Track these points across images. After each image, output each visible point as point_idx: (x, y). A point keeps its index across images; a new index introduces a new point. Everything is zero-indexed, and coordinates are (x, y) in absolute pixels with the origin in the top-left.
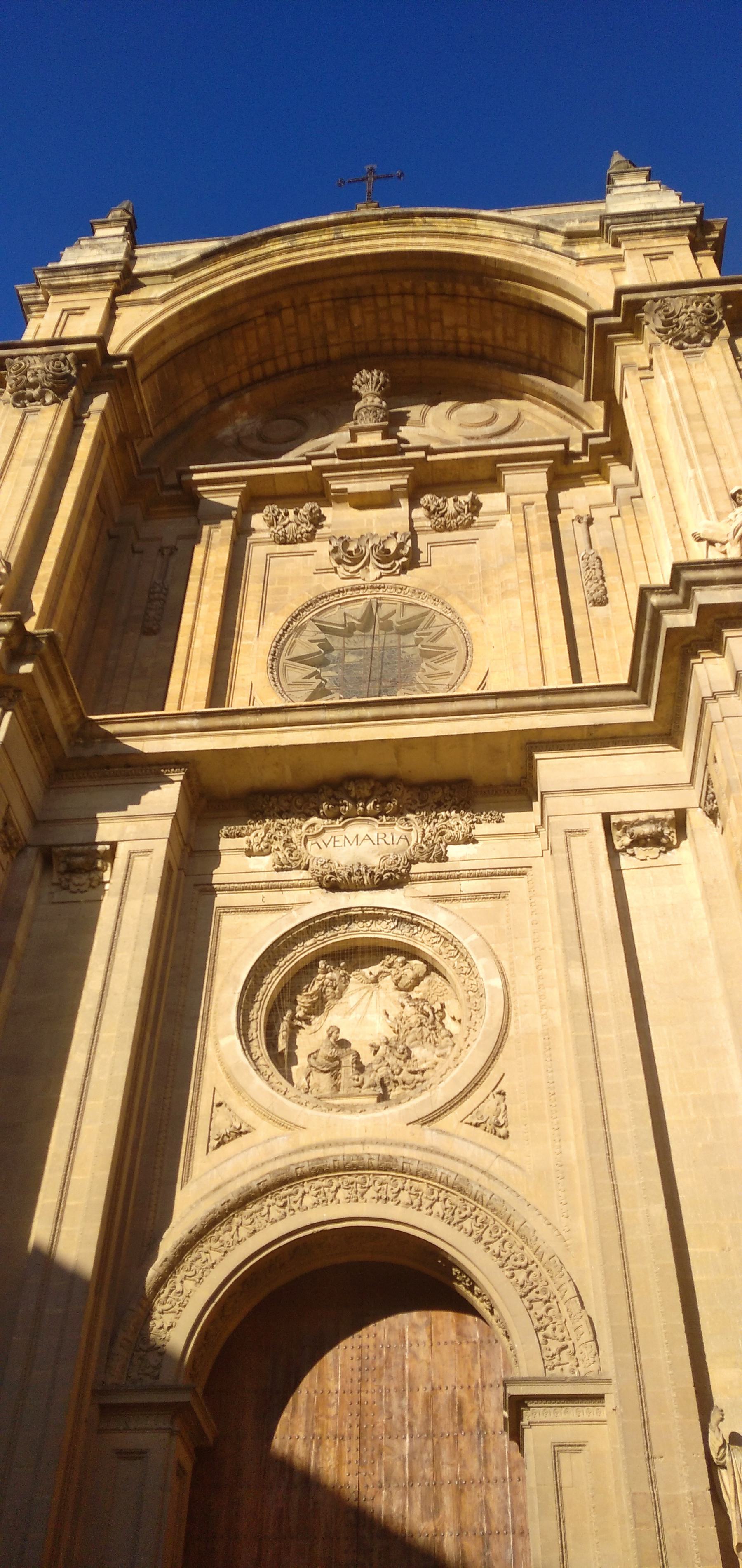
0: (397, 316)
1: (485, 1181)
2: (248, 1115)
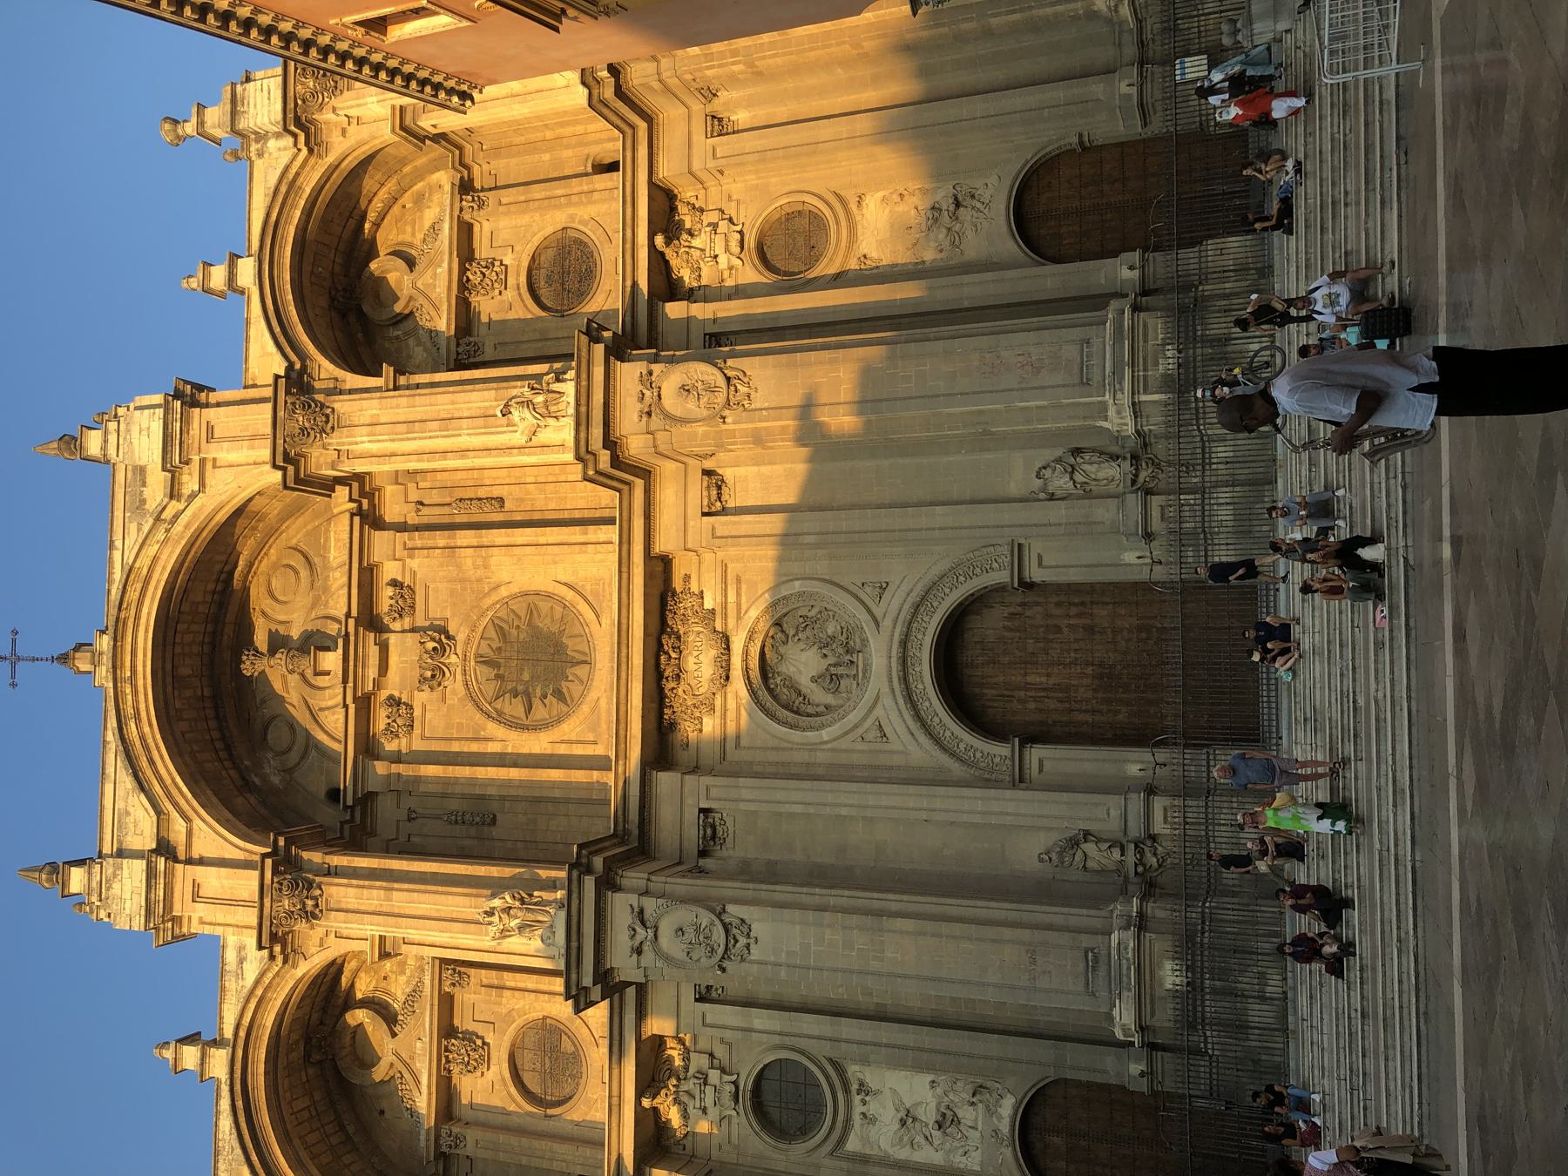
0: (188, 638)
1: (913, 594)
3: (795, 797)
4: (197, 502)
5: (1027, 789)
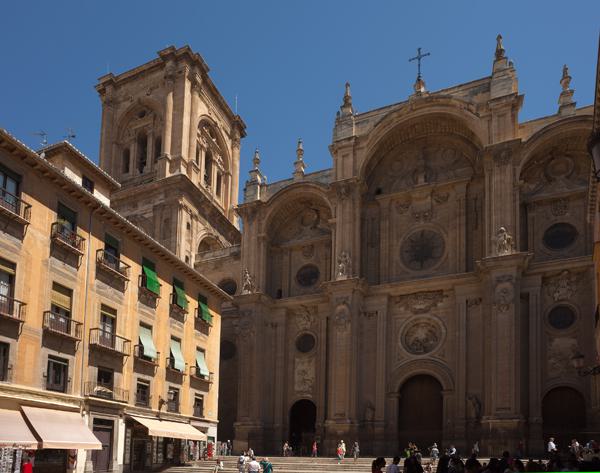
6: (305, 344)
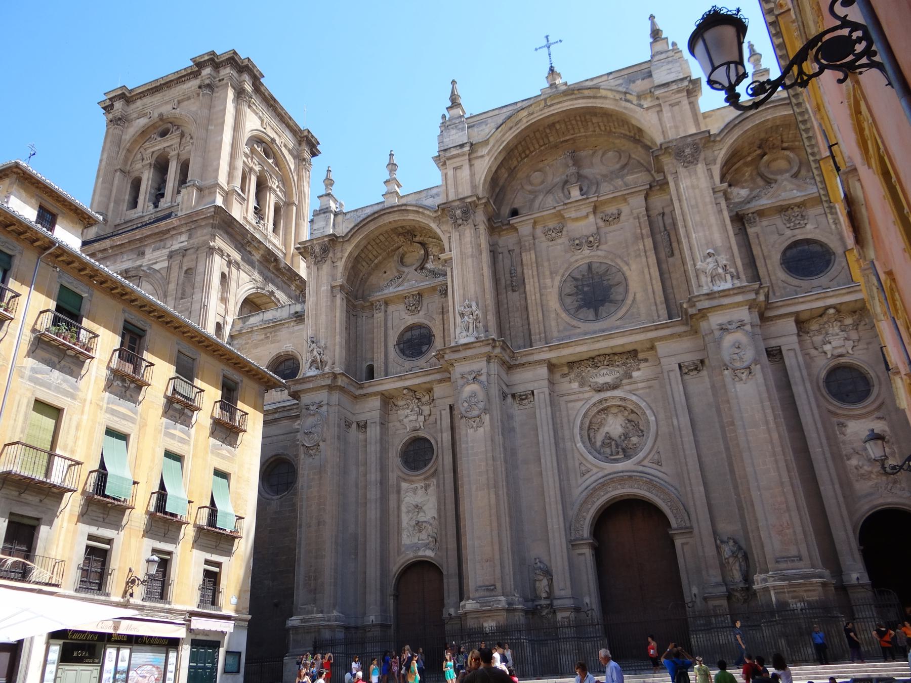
2: (589, 466)
3: (545, 435)
4: (638, 109)
5: (568, 549)
6: (418, 453)
